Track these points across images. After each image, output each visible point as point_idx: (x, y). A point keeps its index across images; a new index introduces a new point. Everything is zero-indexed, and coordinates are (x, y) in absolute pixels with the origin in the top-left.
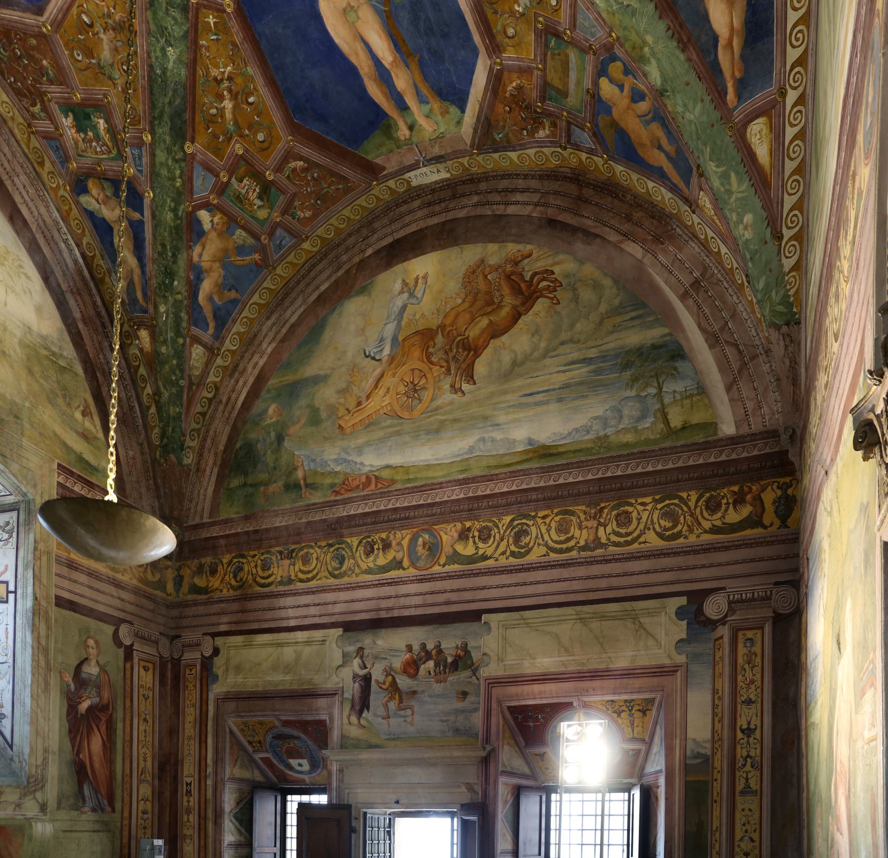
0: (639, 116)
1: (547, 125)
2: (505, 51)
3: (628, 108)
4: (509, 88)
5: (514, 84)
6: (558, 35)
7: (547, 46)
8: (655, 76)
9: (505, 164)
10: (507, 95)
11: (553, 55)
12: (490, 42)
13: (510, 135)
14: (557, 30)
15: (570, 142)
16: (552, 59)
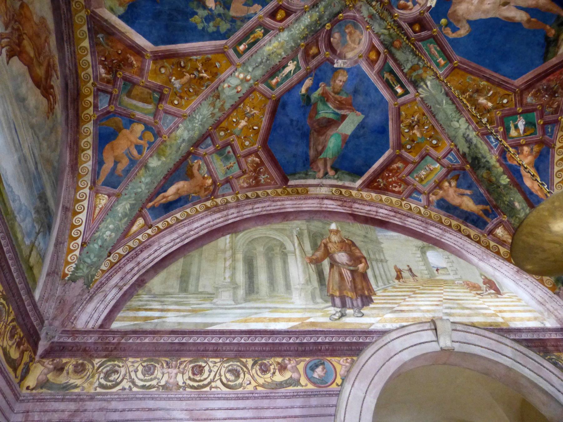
0: (128, 149)
1: (108, 76)
2: (154, 63)
3: (131, 142)
4: (132, 58)
5: (134, 62)
6: (161, 100)
7: (154, 91)
8: (154, 163)
9: (78, 34)
10: (129, 56)
11: (150, 94)
12: (159, 56)
13: (102, 48)
14: (163, 100)
15: (98, 92)
16: (148, 93)
